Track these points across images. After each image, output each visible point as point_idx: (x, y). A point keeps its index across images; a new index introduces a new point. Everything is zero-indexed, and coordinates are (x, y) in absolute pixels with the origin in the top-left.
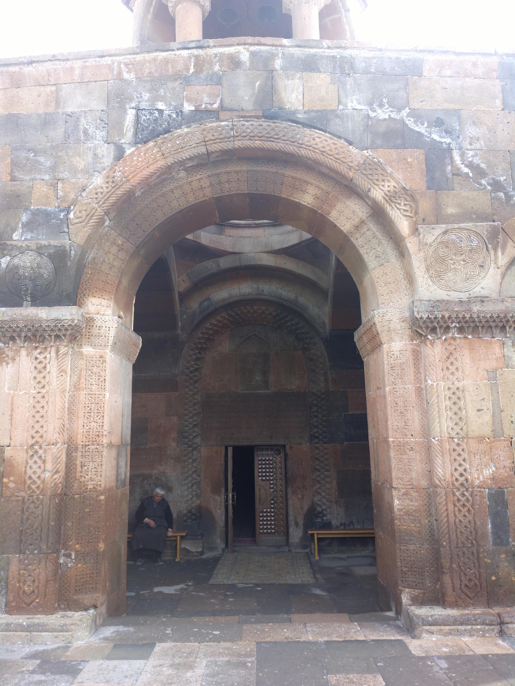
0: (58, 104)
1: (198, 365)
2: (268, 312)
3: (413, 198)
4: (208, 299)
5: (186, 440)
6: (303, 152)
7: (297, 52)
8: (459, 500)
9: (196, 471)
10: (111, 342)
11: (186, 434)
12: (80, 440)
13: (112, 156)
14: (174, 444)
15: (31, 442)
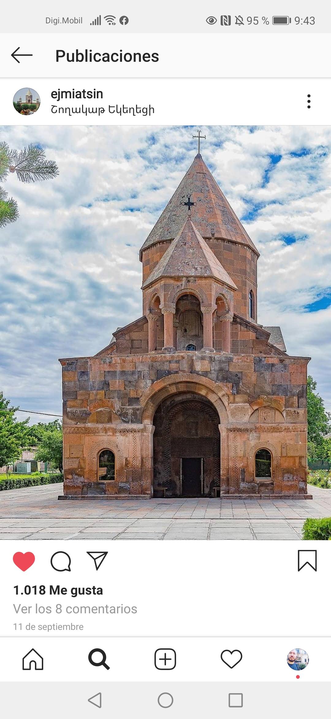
0: (136, 368)
1: (169, 426)
2: (198, 405)
3: (228, 396)
4: (174, 400)
5: (166, 455)
6: (200, 383)
7: (200, 355)
8: (234, 471)
9: (169, 467)
10: (150, 432)
11: (165, 453)
12: (144, 456)
13: (150, 383)
14: (161, 457)
15: (133, 457)
